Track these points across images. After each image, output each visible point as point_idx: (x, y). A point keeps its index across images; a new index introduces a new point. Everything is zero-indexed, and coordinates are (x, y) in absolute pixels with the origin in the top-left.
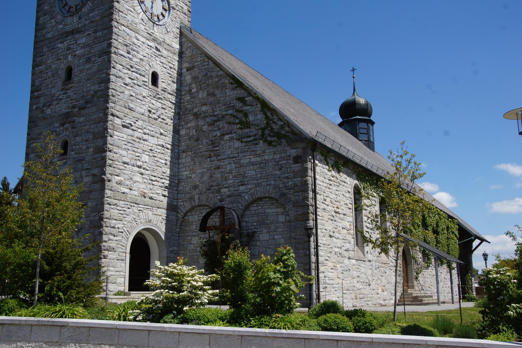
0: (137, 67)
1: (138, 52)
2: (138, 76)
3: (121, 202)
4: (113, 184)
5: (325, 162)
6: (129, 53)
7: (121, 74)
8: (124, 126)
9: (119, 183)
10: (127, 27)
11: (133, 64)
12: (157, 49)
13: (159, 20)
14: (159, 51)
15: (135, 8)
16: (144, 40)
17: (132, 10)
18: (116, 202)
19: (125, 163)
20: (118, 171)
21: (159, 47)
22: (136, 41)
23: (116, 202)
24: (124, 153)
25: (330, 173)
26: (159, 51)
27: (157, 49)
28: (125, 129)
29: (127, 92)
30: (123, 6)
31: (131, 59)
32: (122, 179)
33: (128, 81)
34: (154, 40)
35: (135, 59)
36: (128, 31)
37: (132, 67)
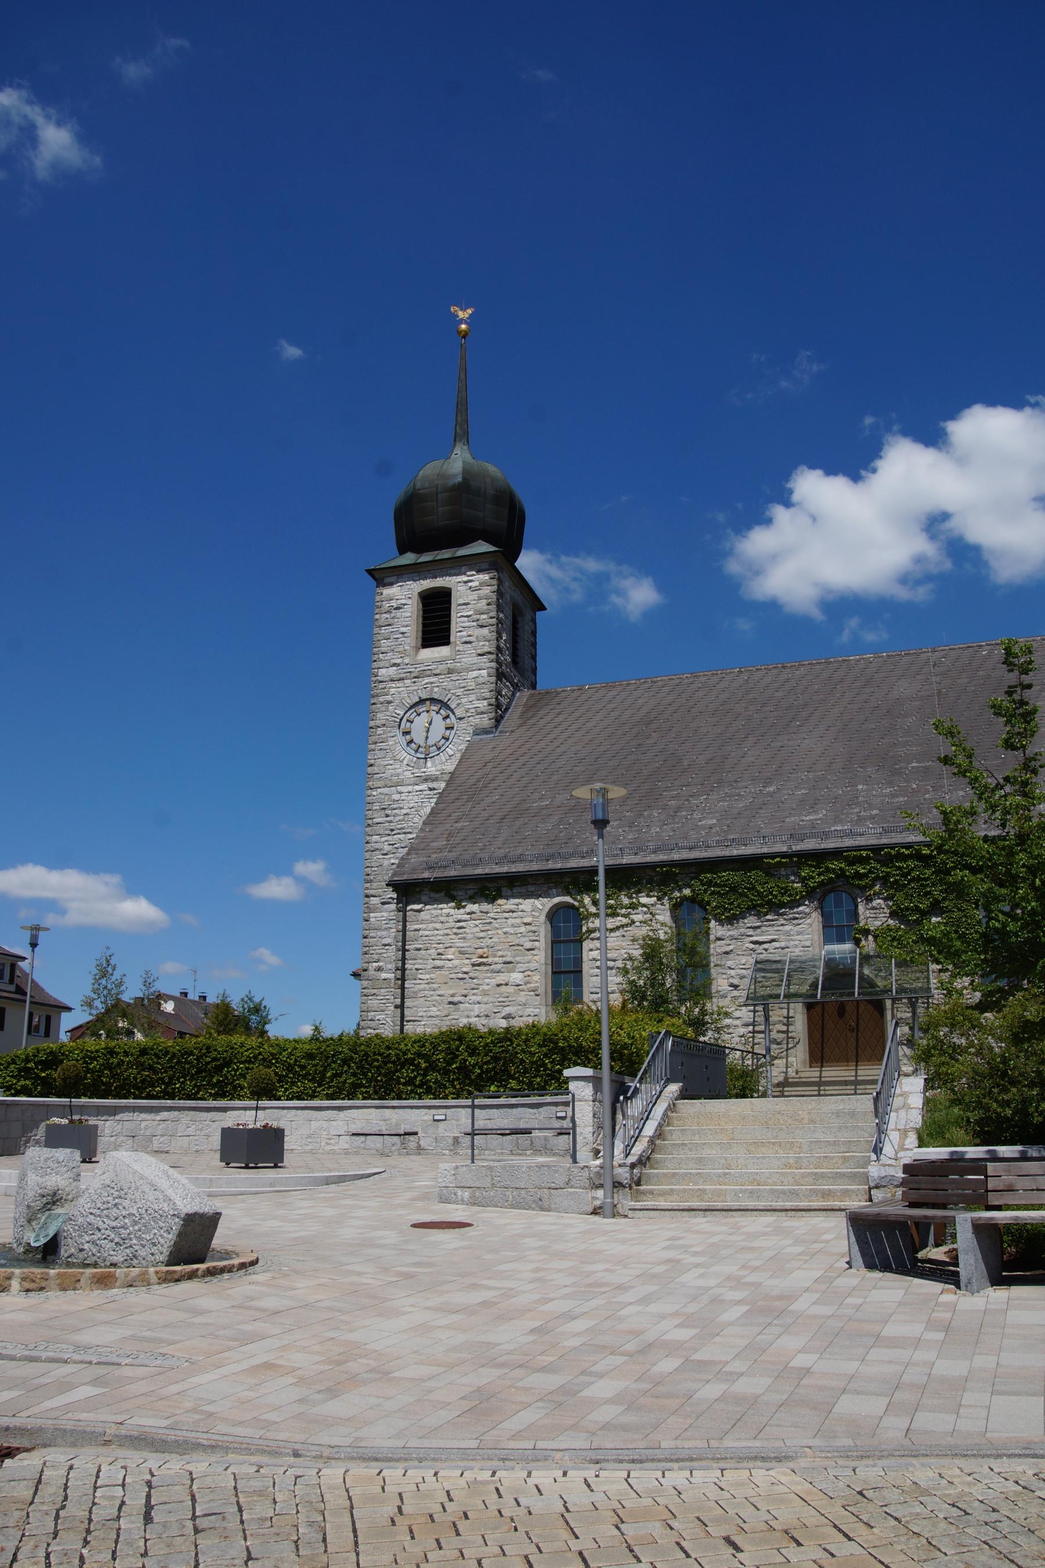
0: (399, 826)
1: (401, 808)
2: (401, 836)
3: (383, 990)
4: (371, 972)
5: (447, 899)
6: (387, 816)
7: (377, 846)
8: (383, 903)
9: (379, 969)
10: (386, 786)
11: (393, 826)
12: (431, 789)
13: (439, 749)
14: (435, 789)
15: (398, 757)
16: (410, 788)
17: (391, 762)
18: (375, 991)
19: (385, 945)
20: (376, 957)
21: (431, 785)
22: (396, 797)
23: (375, 991)
24: (384, 933)
25: (462, 911)
26: (435, 789)
27: (431, 789)
28: (386, 906)
29: (386, 863)
30: (380, 765)
31: (390, 822)
32: (380, 964)
33: (387, 848)
34: (426, 780)
35: (398, 818)
36: (386, 790)
37: (392, 830)
